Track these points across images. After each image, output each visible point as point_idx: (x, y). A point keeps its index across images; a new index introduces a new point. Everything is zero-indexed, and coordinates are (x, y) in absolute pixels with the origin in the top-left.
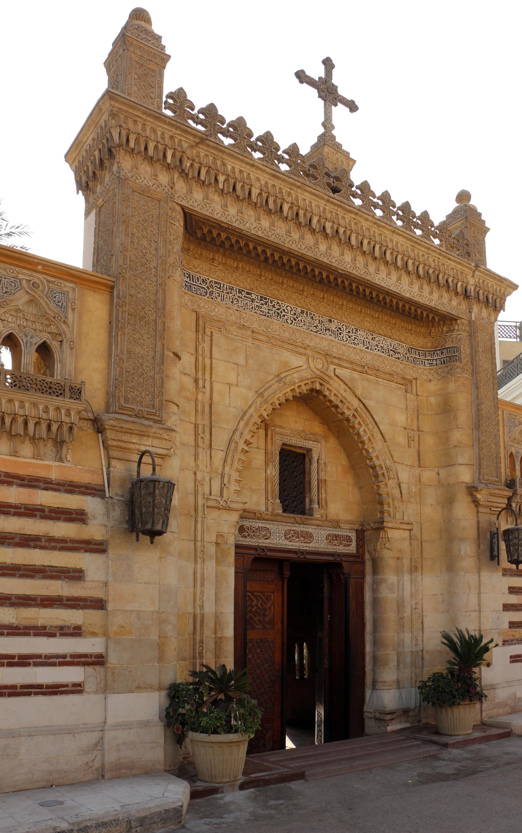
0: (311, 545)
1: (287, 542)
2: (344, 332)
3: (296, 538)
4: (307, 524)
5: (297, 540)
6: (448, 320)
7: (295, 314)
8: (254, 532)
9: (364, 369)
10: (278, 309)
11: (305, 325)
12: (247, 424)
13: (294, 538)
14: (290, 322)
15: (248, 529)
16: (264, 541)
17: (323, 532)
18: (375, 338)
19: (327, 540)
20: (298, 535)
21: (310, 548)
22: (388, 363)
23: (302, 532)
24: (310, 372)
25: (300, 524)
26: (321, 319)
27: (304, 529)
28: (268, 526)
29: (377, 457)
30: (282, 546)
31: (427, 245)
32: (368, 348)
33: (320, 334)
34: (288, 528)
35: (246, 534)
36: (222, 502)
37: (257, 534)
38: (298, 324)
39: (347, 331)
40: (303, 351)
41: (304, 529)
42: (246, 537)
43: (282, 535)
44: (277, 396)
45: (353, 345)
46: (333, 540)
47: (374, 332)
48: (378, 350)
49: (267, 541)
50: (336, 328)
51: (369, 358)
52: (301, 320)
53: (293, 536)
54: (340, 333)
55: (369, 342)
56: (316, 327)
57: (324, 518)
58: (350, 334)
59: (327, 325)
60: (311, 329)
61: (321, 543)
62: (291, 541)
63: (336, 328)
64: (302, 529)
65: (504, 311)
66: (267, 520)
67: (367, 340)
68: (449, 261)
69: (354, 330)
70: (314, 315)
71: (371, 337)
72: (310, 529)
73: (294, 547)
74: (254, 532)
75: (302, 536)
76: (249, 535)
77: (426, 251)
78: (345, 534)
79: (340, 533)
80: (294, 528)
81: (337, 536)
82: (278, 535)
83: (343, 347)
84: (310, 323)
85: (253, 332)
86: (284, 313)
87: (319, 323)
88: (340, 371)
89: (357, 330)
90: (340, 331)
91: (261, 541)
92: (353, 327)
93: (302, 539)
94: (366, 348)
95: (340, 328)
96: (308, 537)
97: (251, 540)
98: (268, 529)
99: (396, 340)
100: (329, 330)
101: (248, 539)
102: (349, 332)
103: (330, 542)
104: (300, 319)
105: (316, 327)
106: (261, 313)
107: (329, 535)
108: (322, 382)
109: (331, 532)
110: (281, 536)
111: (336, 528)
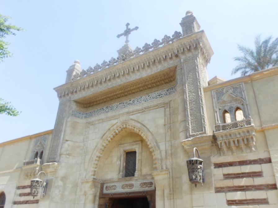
0: (132, 189)
4: (131, 181)
5: (127, 188)
6: (174, 70)
8: (110, 188)
9: (142, 111)
12: (97, 151)
17: (138, 183)
22: (155, 102)
23: (129, 184)
24: (120, 122)
25: (128, 181)
28: (116, 184)
29: (150, 143)
34: (124, 183)
40: (118, 117)
42: (107, 190)
44: (108, 137)
46: (143, 185)
47: (149, 93)
49: (115, 190)
51: (145, 105)
53: (125, 187)
59: (128, 103)
62: (124, 189)
64: (129, 183)
66: (116, 182)
72: (133, 182)
74: (110, 188)
75: (129, 186)
78: (149, 181)
79: (146, 182)
81: (145, 183)
85: (102, 120)
88: (132, 117)
89: (141, 97)
91: (112, 191)
92: (140, 97)
93: (129, 187)
95: (134, 101)
96: (131, 186)
98: (115, 185)
99: (160, 90)
100: (129, 104)
101: (108, 191)
107: (141, 183)
108: (125, 124)
109: (142, 182)
110: (120, 188)
111: (145, 179)
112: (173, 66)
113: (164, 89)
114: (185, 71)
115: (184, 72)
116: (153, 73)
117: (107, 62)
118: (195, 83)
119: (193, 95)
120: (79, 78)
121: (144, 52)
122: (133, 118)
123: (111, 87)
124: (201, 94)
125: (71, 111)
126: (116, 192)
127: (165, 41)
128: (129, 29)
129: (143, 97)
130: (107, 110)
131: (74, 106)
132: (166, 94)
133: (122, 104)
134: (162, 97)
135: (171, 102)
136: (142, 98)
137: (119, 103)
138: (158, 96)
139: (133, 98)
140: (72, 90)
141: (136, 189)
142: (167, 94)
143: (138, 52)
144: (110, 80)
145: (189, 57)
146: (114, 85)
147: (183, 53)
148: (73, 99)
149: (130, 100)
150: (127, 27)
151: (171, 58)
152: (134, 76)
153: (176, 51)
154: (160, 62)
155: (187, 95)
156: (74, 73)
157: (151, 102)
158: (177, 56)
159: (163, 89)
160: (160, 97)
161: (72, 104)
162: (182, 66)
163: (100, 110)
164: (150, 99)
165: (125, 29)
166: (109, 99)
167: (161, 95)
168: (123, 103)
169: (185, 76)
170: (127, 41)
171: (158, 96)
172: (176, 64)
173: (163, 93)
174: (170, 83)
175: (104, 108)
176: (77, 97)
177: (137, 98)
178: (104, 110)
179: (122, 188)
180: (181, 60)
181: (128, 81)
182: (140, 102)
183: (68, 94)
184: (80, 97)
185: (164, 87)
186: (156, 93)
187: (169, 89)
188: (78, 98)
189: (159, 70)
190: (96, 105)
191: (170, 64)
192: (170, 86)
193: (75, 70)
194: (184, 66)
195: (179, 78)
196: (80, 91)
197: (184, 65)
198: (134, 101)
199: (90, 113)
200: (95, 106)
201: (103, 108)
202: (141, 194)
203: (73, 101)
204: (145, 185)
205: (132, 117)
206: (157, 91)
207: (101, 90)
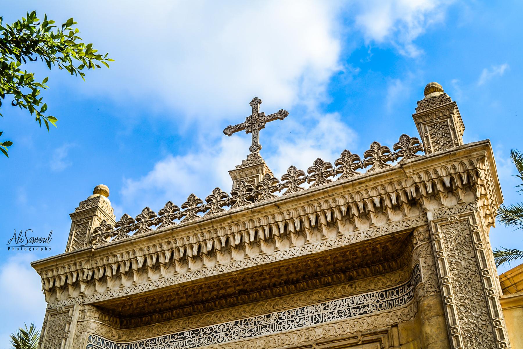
2: (286, 320)
6: (403, 241)
7: (227, 330)
10: (210, 334)
11: (238, 335)
14: (220, 340)
18: (328, 306)
26: (257, 319)
31: (321, 191)
33: (256, 335)
38: (229, 338)
39: (290, 316)
45: (298, 328)
47: (327, 299)
48: (333, 317)
50: (275, 320)
52: (234, 332)
54: (280, 324)
55: (319, 315)
56: (251, 331)
58: (293, 319)
59: (263, 323)
60: (244, 335)
63: (275, 320)
67: (316, 313)
68: (363, 185)
69: (300, 311)
71: (322, 307)
77: (326, 195)
83: (283, 337)
84: (244, 330)
86: (215, 334)
87: (255, 325)
89: (303, 310)
92: (297, 309)
94: (315, 323)
95: (280, 318)
100: (266, 326)
104: (232, 332)
105: (251, 331)
106: (192, 346)
112: (403, 228)
113: (373, 290)
114: (443, 248)
115: (440, 248)
116: (344, 243)
117: (199, 201)
118: (475, 282)
119: (472, 316)
120: (110, 240)
121: (312, 183)
123: (215, 273)
124: (497, 315)
125: (85, 336)
127: (375, 159)
128: (261, 115)
129: (309, 310)
130: (195, 341)
131: (94, 324)
132: (378, 305)
133: (244, 326)
134: (365, 312)
135: (395, 330)
136: (305, 313)
137: (232, 323)
138: (353, 308)
139: (277, 310)
140: (90, 273)
142: (381, 306)
143: (295, 181)
144: (212, 253)
145: (450, 209)
146: (226, 271)
147: (434, 196)
148: (93, 301)
149: (268, 317)
150: (255, 109)
151: (397, 207)
152: (287, 249)
153: (413, 190)
154: (365, 215)
155: (456, 316)
156: (96, 224)
157: (336, 326)
158: (414, 203)
159: (369, 291)
160: (362, 311)
161: (88, 314)
162: (434, 231)
163: (173, 337)
164: (331, 316)
165: (249, 112)
166: (200, 307)
167: (364, 307)
168: (247, 324)
169: (442, 260)
170: (255, 147)
171: (353, 308)
172: (413, 226)
173: (370, 301)
174: (387, 276)
175: (185, 334)
176: (103, 293)
177: (289, 310)
178: (184, 339)
180: (426, 214)
181: (267, 261)
182: (301, 323)
183: (76, 285)
184: (116, 296)
185: (373, 287)
186: (349, 299)
187: (386, 291)
188: (108, 298)
189: (362, 238)
190: (158, 322)
191: (396, 222)
192: (389, 283)
193: (98, 213)
194: (437, 231)
195: (425, 265)
196: (118, 276)
197: (439, 230)
198: (280, 318)
199: (141, 344)
200: (157, 324)
201: (182, 334)
203: (92, 304)
206: (351, 294)
207: (183, 280)
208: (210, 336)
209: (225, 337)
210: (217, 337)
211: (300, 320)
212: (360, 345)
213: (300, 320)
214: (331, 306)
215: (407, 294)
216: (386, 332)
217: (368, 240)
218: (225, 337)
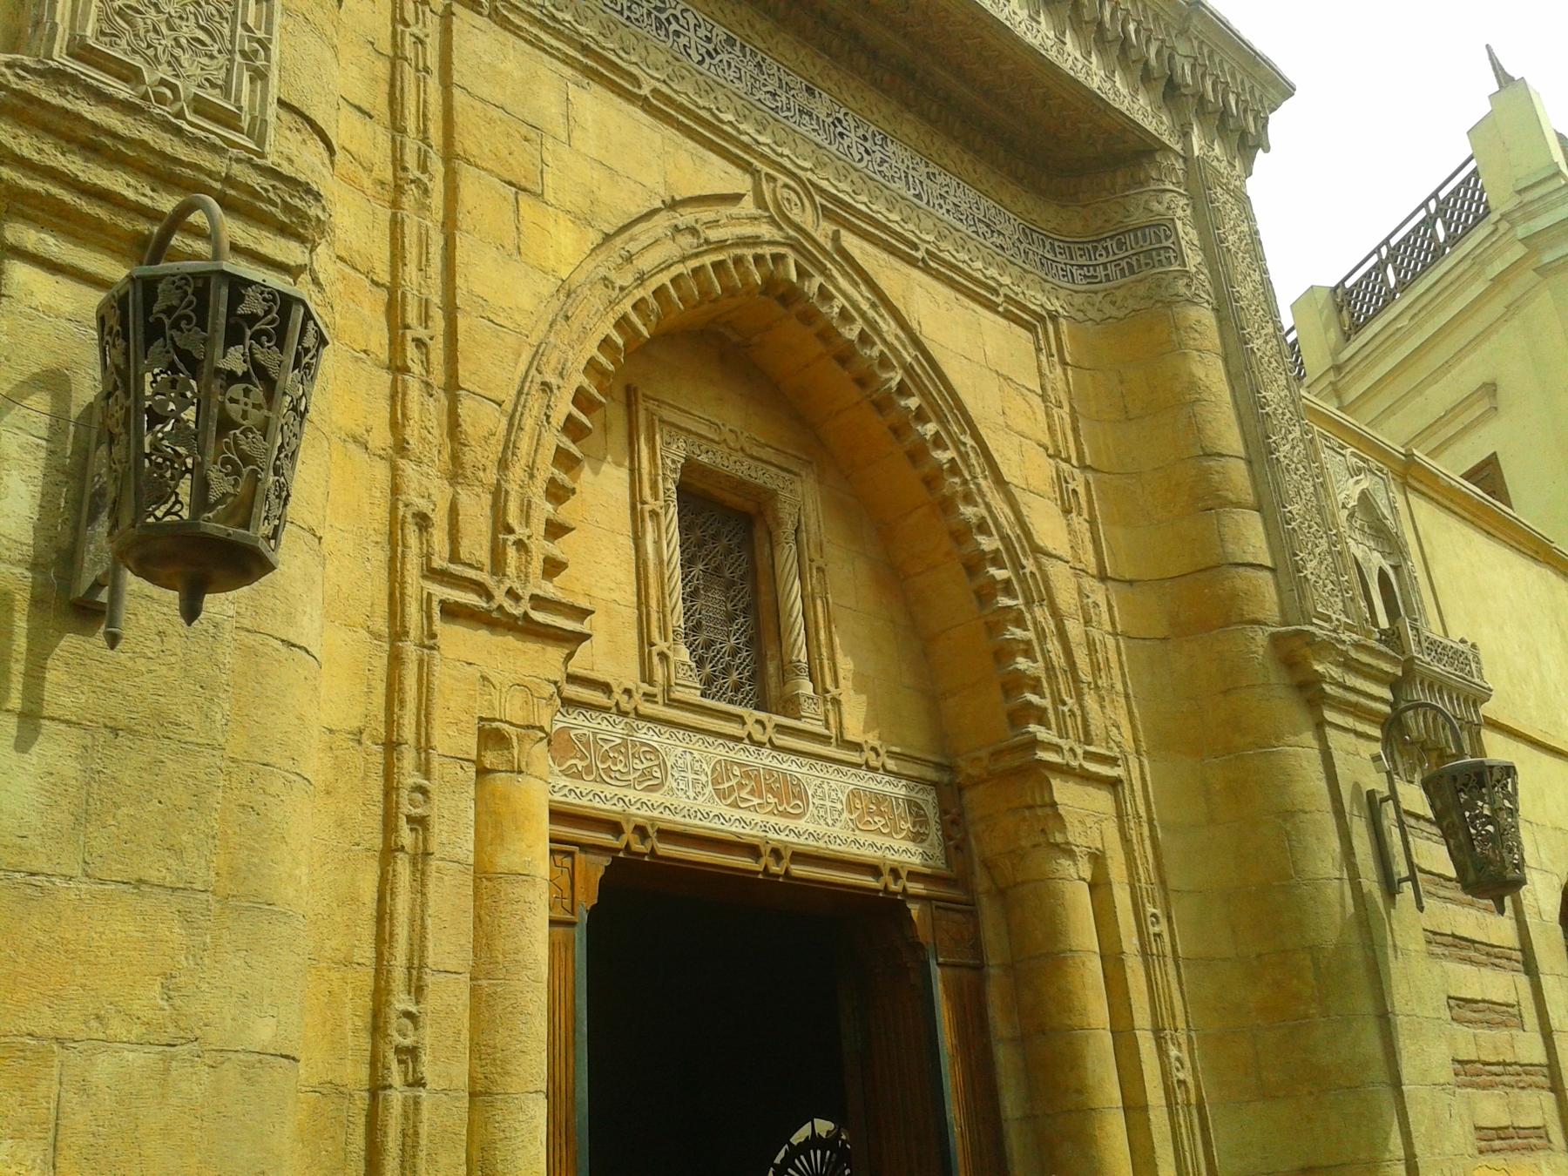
0: (802, 824)
1: (721, 808)
3: (752, 792)
5: (756, 801)
6: (1130, 153)
13: (744, 794)
15: (587, 745)
16: (645, 797)
19: (851, 812)
20: (758, 782)
21: (798, 835)
23: (770, 772)
25: (761, 744)
27: (775, 763)
30: (706, 823)
32: (918, 196)
35: (580, 765)
36: (500, 598)
37: (620, 767)
41: (775, 763)
42: (579, 776)
43: (703, 778)
49: (656, 797)
50: (828, 115)
53: (741, 786)
57: (833, 732)
58: (867, 145)
61: (835, 821)
62: (735, 805)
63: (828, 115)
65: (1267, 149)
70: (764, 60)
73: (747, 831)
75: (770, 790)
76: (588, 770)
80: (742, 757)
82: (691, 776)
90: (840, 129)
91: (631, 794)
93: (772, 800)
97: (597, 788)
100: (811, 116)
101: (584, 786)
102: (865, 139)
103: (860, 818)
122: (856, 254)
126: (667, 815)
141: (822, 829)
179: (722, 795)
191: (1138, 107)
202: (868, 881)
204: (881, 814)
205: (850, 242)
208: (663, 17)
209: (708, 60)
210: (683, 40)
211: (883, 161)
212: (998, 313)
213: (883, 161)
214: (940, 179)
215: (1081, 267)
216: (1041, 319)
217: (1102, 99)
218: (708, 60)
